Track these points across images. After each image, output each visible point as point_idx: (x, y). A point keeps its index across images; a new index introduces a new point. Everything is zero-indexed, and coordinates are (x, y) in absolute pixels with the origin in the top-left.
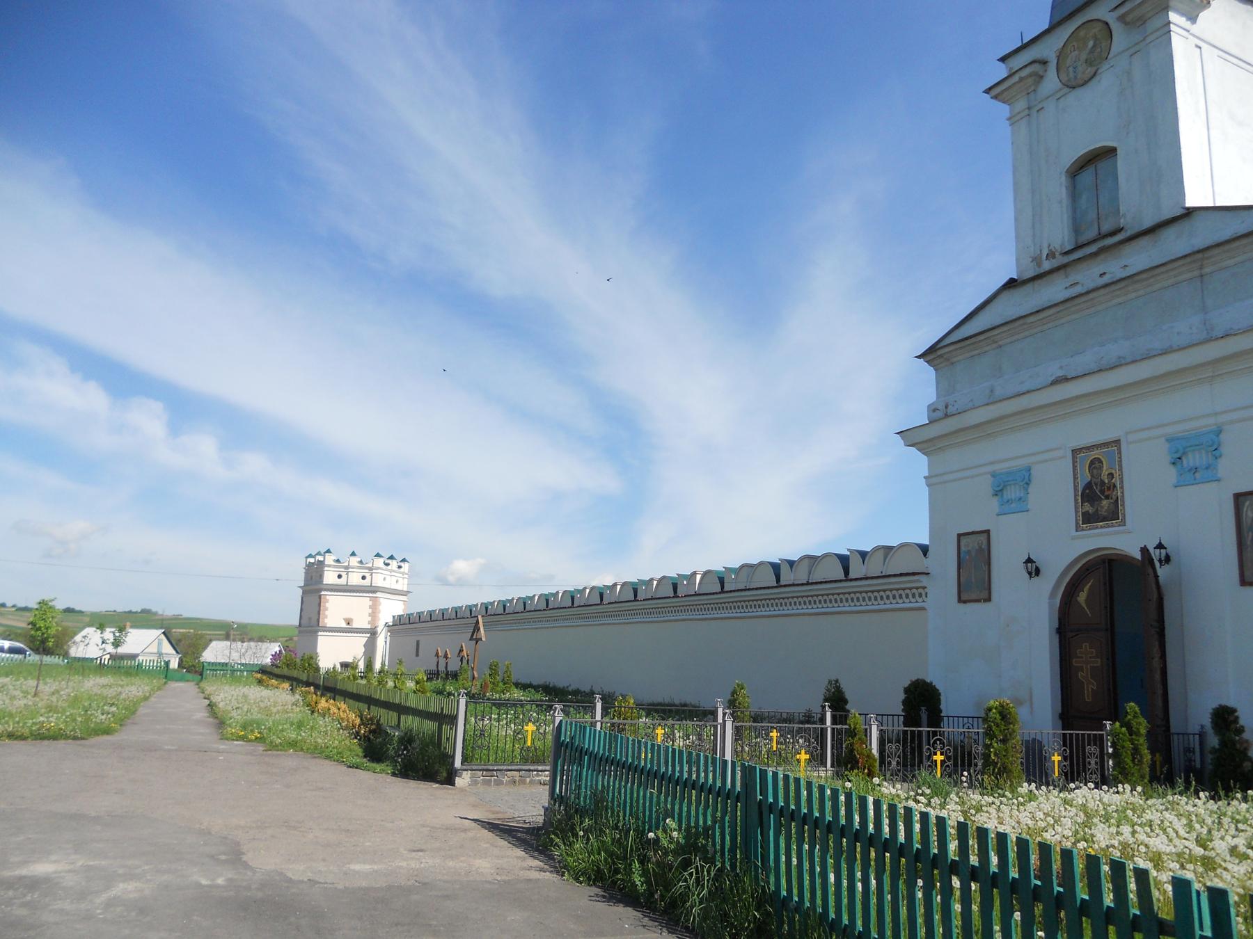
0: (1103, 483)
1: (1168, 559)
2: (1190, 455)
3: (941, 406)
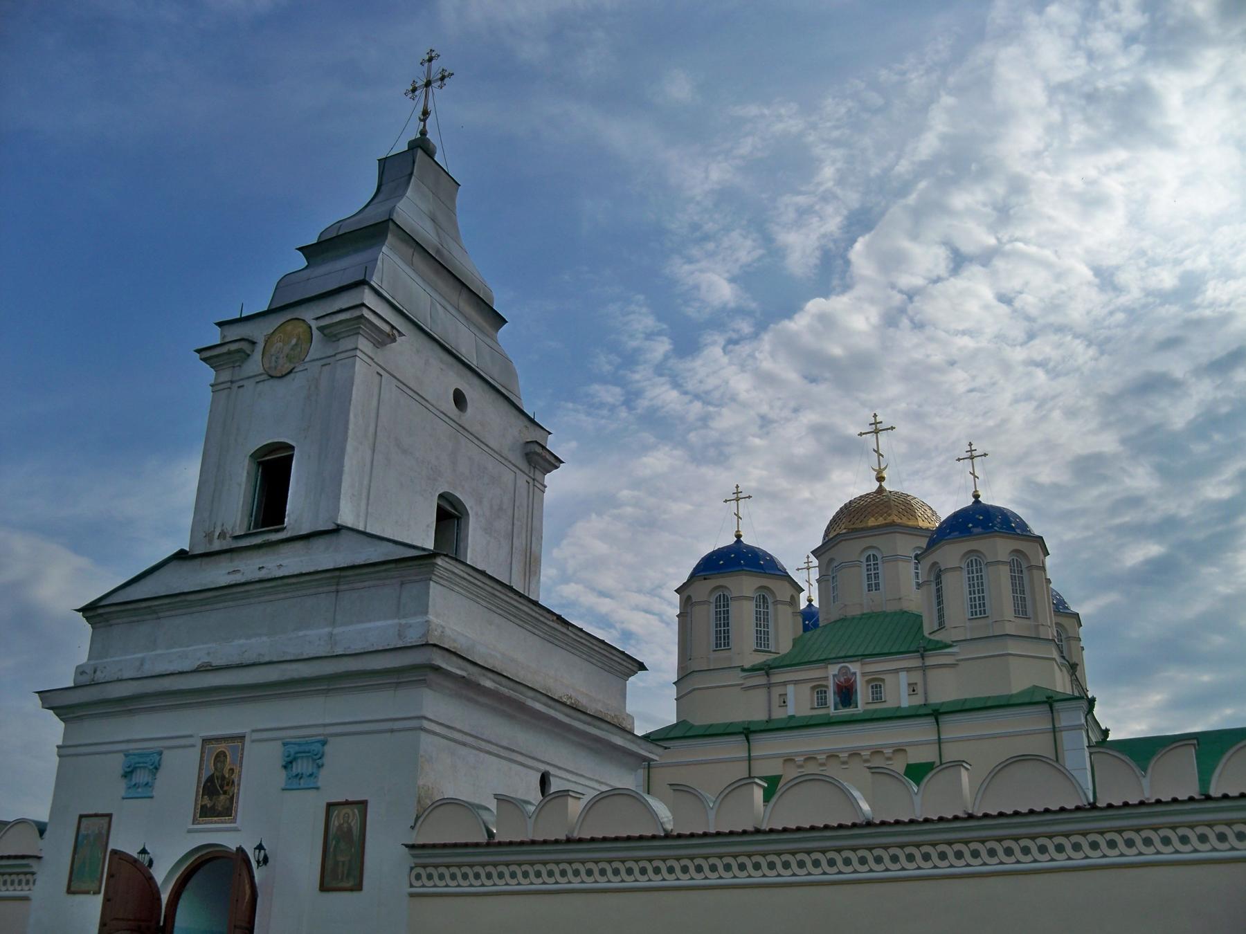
0: (223, 778)
1: (266, 860)
2: (299, 761)
3: (89, 671)
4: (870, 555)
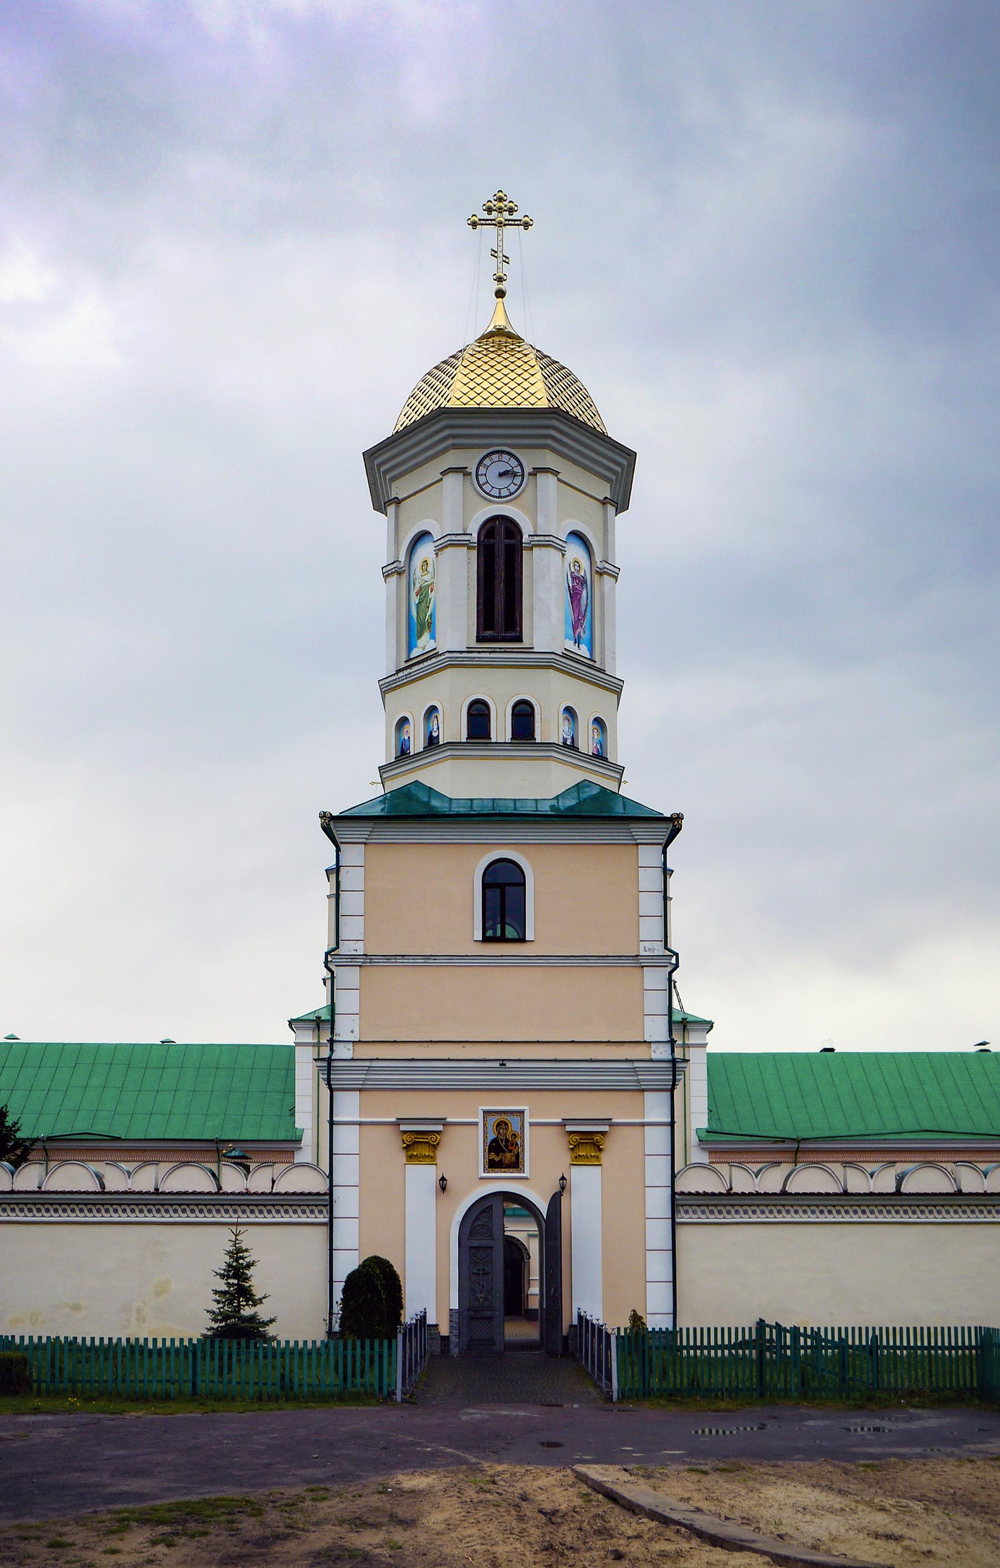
0: (507, 1141)
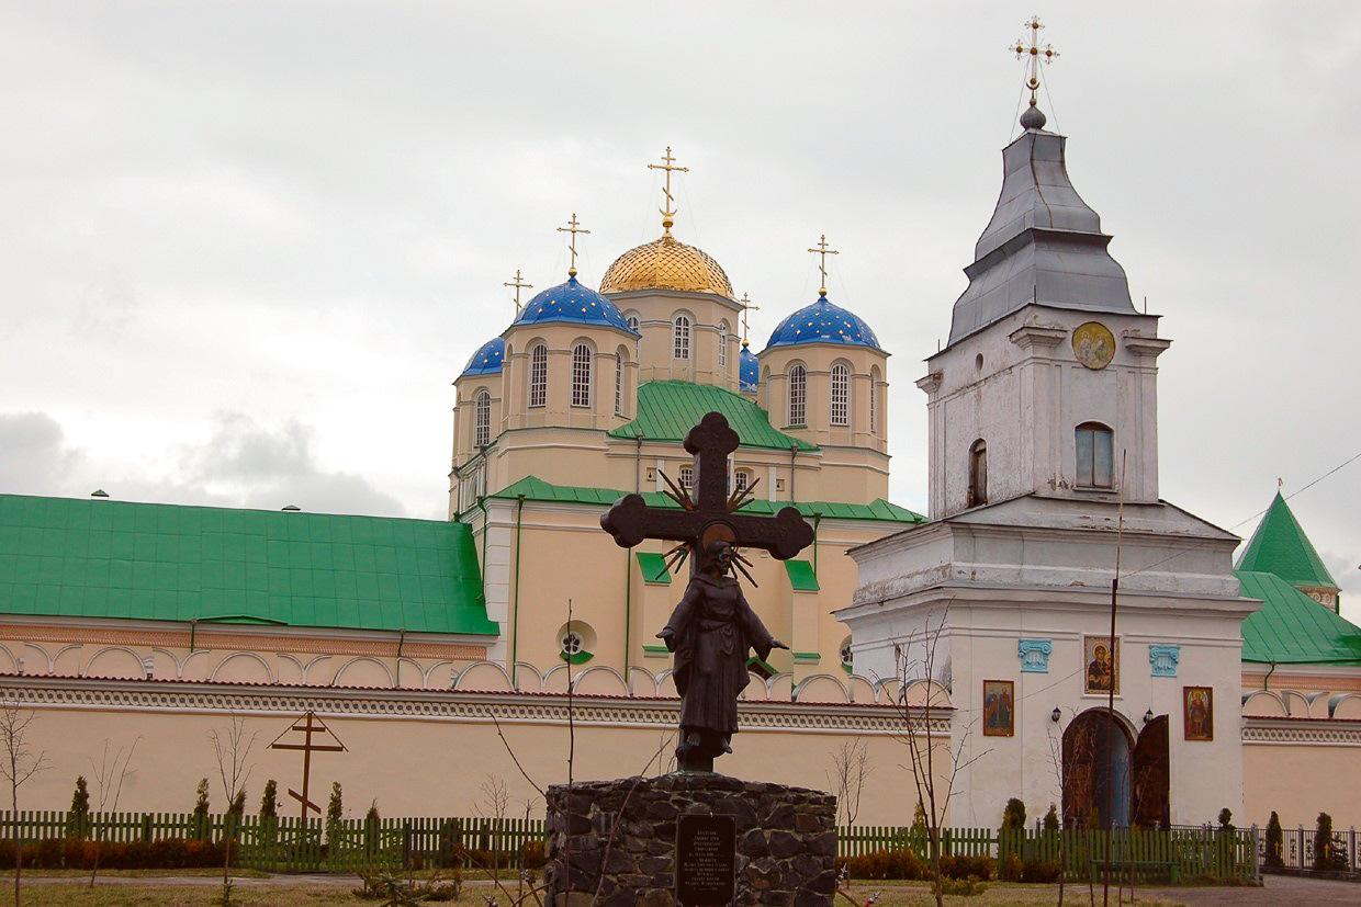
0: (1104, 664)
4: (680, 319)
